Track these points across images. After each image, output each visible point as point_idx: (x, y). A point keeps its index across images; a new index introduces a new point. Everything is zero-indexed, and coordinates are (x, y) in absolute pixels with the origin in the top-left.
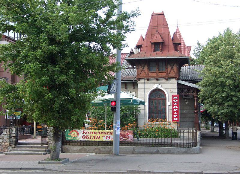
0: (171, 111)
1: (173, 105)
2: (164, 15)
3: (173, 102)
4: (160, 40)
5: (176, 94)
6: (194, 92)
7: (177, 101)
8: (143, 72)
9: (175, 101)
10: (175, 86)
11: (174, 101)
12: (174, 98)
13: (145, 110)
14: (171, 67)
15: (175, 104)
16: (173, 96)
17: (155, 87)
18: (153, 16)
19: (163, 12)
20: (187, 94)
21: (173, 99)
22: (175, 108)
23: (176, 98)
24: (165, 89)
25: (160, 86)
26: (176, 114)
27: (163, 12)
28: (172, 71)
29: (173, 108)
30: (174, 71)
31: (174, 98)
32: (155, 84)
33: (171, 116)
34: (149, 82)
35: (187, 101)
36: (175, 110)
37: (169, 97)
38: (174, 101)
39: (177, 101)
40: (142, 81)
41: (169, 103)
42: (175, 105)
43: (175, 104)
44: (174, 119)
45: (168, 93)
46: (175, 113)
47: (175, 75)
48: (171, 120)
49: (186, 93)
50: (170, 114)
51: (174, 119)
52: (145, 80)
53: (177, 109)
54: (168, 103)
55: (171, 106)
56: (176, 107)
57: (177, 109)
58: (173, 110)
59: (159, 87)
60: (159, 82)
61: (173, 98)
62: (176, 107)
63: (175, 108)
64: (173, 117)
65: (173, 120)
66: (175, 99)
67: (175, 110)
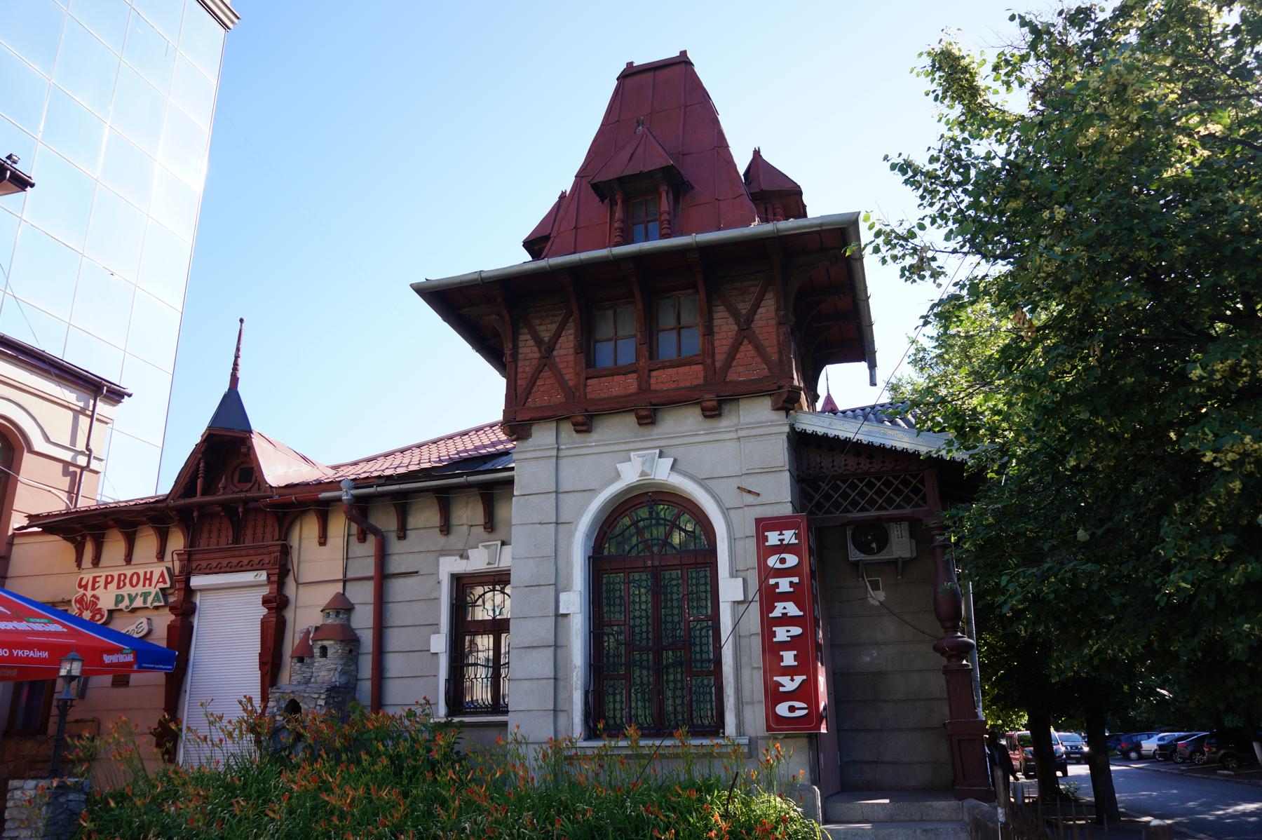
0: (757, 643)
1: (769, 597)
2: (689, 64)
3: (766, 573)
4: (656, 159)
5: (787, 510)
6: (924, 498)
7: (792, 560)
8: (546, 380)
9: (783, 561)
10: (778, 452)
11: (772, 561)
12: (773, 538)
13: (560, 651)
14: (738, 323)
15: (784, 585)
16: (764, 525)
17: (630, 474)
18: (629, 81)
19: (684, 53)
20: (873, 513)
21: (765, 552)
22: (785, 620)
23: (789, 536)
24: (701, 482)
25: (668, 462)
26: (790, 672)
27: (684, 53)
28: (747, 350)
29: (769, 624)
30: (759, 349)
31: (773, 538)
32: (632, 454)
33: (755, 685)
34: (594, 436)
35: (875, 587)
36: (782, 634)
37: (732, 540)
38: (772, 561)
39: (792, 560)
40: (543, 436)
41: (740, 580)
42: (785, 597)
43: (784, 585)
44: (782, 709)
45: (725, 511)
46: (789, 658)
47: (766, 372)
48: (756, 720)
49: (863, 509)
50: (746, 673)
51: (782, 709)
52: (563, 435)
53: (796, 631)
54: (730, 589)
55: (755, 609)
56: (792, 609)
57: (796, 631)
58: (767, 634)
59: (663, 473)
60: (657, 431)
61: (761, 539)
62: (792, 609)
63: (785, 620)
64: (774, 695)
65: (775, 722)
66: (781, 548)
67: (782, 634)
